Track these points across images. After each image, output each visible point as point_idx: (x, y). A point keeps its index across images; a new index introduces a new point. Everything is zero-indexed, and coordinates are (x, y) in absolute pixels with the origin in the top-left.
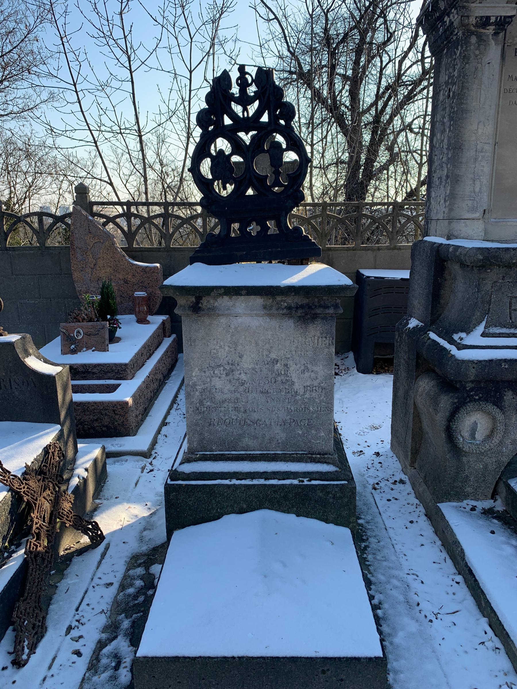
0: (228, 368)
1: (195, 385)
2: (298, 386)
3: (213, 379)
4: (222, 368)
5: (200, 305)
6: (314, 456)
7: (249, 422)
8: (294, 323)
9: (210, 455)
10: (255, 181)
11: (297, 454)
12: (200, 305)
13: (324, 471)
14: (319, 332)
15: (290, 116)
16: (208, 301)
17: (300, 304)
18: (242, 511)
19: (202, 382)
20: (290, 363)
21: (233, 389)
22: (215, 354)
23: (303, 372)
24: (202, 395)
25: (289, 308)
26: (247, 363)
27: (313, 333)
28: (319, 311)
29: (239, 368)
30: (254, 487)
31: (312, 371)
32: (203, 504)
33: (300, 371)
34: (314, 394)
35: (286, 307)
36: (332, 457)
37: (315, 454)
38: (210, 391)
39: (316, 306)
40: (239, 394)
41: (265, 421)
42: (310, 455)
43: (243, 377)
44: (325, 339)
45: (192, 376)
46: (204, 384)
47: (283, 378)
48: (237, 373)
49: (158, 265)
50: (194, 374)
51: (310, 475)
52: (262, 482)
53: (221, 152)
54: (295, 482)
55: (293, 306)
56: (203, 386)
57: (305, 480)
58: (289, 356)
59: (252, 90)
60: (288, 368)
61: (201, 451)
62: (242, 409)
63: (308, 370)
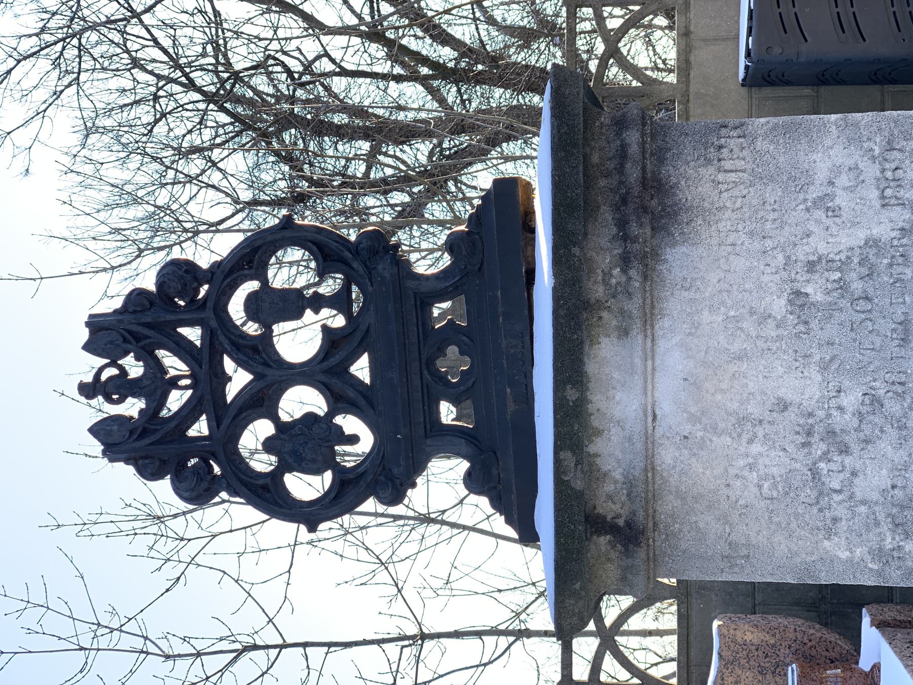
0: (823, 446)
1: (879, 554)
2: (884, 226)
3: (859, 496)
4: (822, 465)
5: (621, 522)
8: (674, 245)
10: (333, 361)
12: (621, 522)
14: (702, 171)
15: (186, 271)
16: (610, 497)
17: (614, 230)
19: (868, 530)
20: (802, 253)
21: (892, 433)
22: (775, 486)
23: (834, 212)
25: (625, 261)
26: (805, 388)
27: (705, 189)
28: (633, 173)
31: (831, 183)
33: (829, 222)
35: (624, 271)
38: (902, 507)
39: (621, 183)
43: (851, 400)
44: (724, 151)
45: (850, 560)
46: (877, 524)
47: (854, 275)
48: (839, 421)
49: (716, 624)
50: (844, 555)
53: (269, 446)
55: (620, 251)
56: (885, 528)
58: (781, 258)
59: (134, 368)
60: (820, 259)
63: (831, 197)
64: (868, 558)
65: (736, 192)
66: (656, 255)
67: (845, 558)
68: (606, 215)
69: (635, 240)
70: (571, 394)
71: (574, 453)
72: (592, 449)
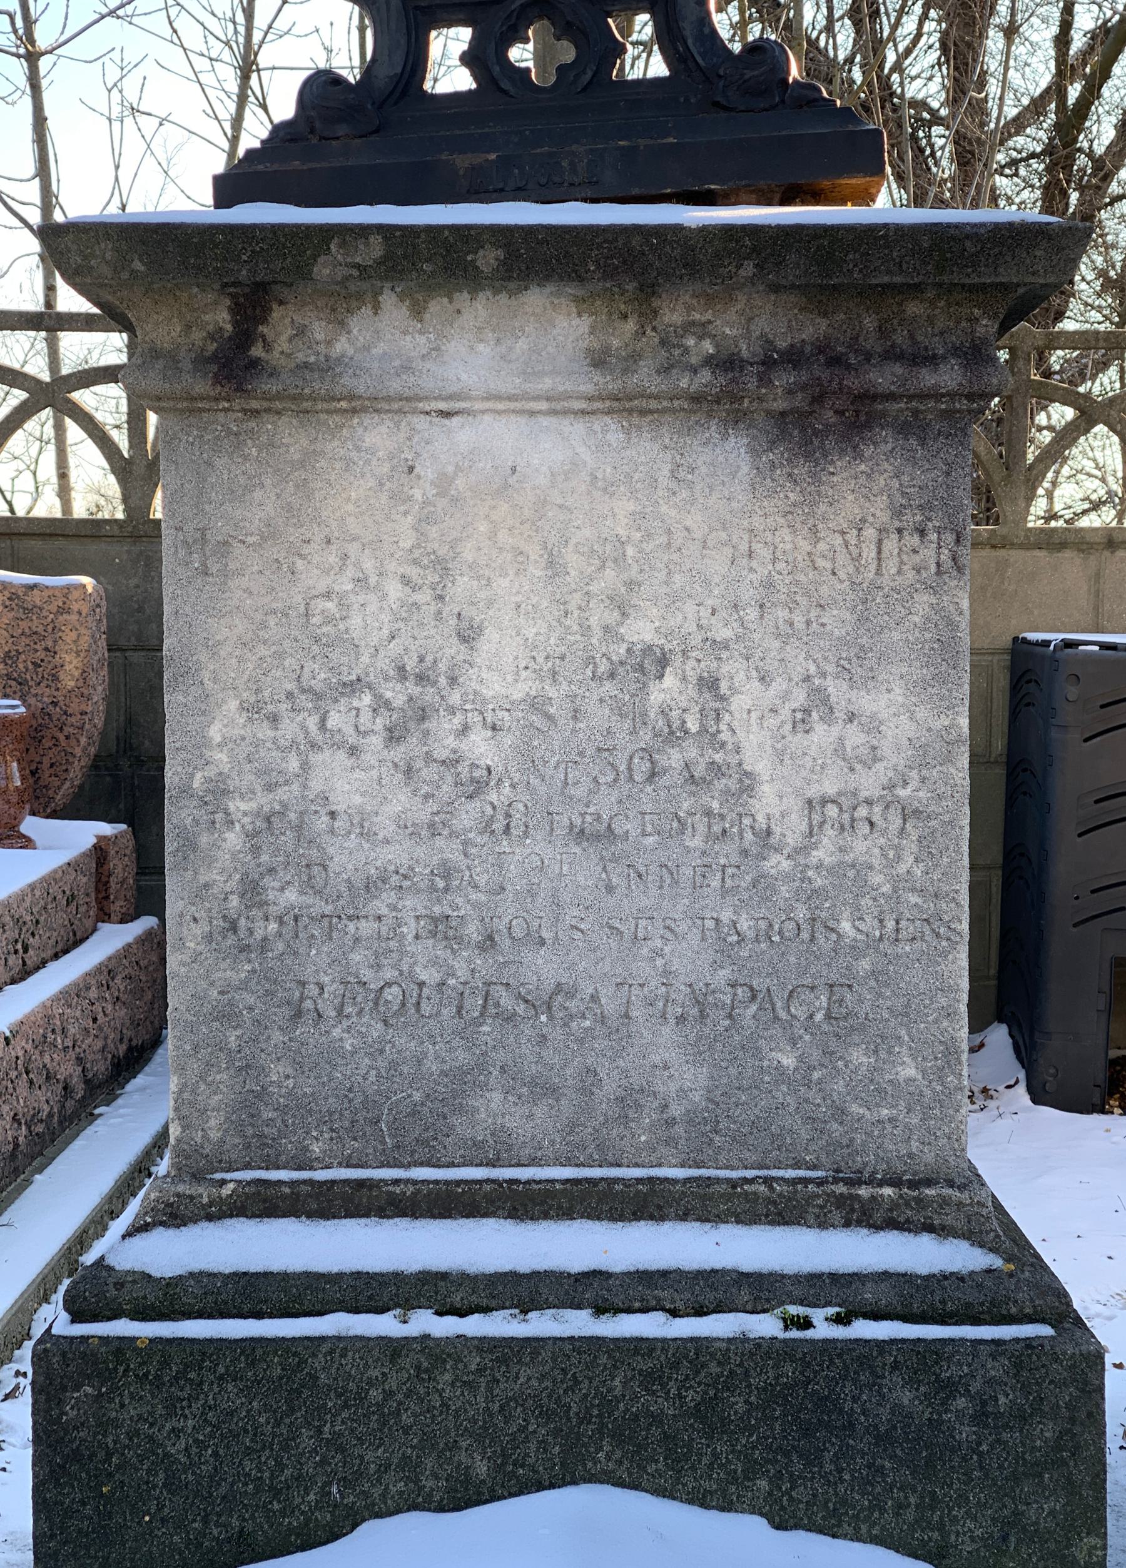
0: (399, 701)
3: (316, 758)
4: (367, 699)
5: (257, 351)
6: (864, 1192)
7: (506, 1000)
8: (754, 452)
9: (293, 1183)
11: (767, 1181)
12: (257, 351)
13: (924, 1271)
14: (882, 501)
16: (301, 332)
17: (782, 344)
18: (462, 1496)
19: (258, 773)
20: (733, 670)
21: (423, 813)
22: (329, 620)
24: (256, 850)
25: (726, 363)
26: (500, 672)
27: (850, 506)
28: (883, 377)
29: (455, 698)
30: (535, 1353)
31: (851, 717)
32: (248, 1451)
33: (785, 713)
34: (862, 846)
36: (964, 1197)
37: (870, 1182)
38: (299, 828)
39: (868, 357)
40: (456, 845)
41: (594, 998)
42: (841, 1189)
43: (480, 748)
45: (206, 742)
46: (270, 788)
47: (693, 753)
48: (444, 726)
49: (87, 580)
50: (215, 733)
51: (849, 1293)
52: (578, 1323)
54: (765, 1326)
55: (745, 354)
56: (264, 800)
57: (818, 1315)
58: (725, 633)
60: (722, 698)
61: (248, 1166)
62: (473, 931)
64: (211, 772)
65: (842, 558)
66: (737, 419)
67: (210, 740)
68: (811, 329)
69: (764, 380)
70: (488, 258)
71: (380, 262)
72: (388, 299)
